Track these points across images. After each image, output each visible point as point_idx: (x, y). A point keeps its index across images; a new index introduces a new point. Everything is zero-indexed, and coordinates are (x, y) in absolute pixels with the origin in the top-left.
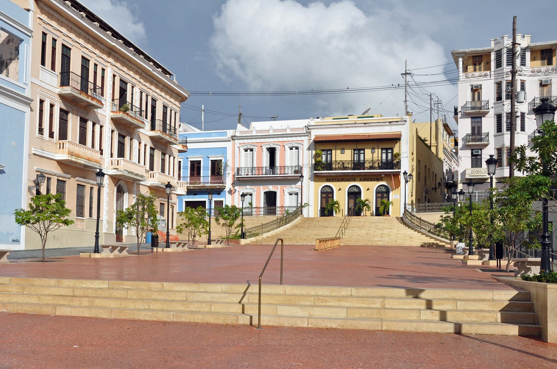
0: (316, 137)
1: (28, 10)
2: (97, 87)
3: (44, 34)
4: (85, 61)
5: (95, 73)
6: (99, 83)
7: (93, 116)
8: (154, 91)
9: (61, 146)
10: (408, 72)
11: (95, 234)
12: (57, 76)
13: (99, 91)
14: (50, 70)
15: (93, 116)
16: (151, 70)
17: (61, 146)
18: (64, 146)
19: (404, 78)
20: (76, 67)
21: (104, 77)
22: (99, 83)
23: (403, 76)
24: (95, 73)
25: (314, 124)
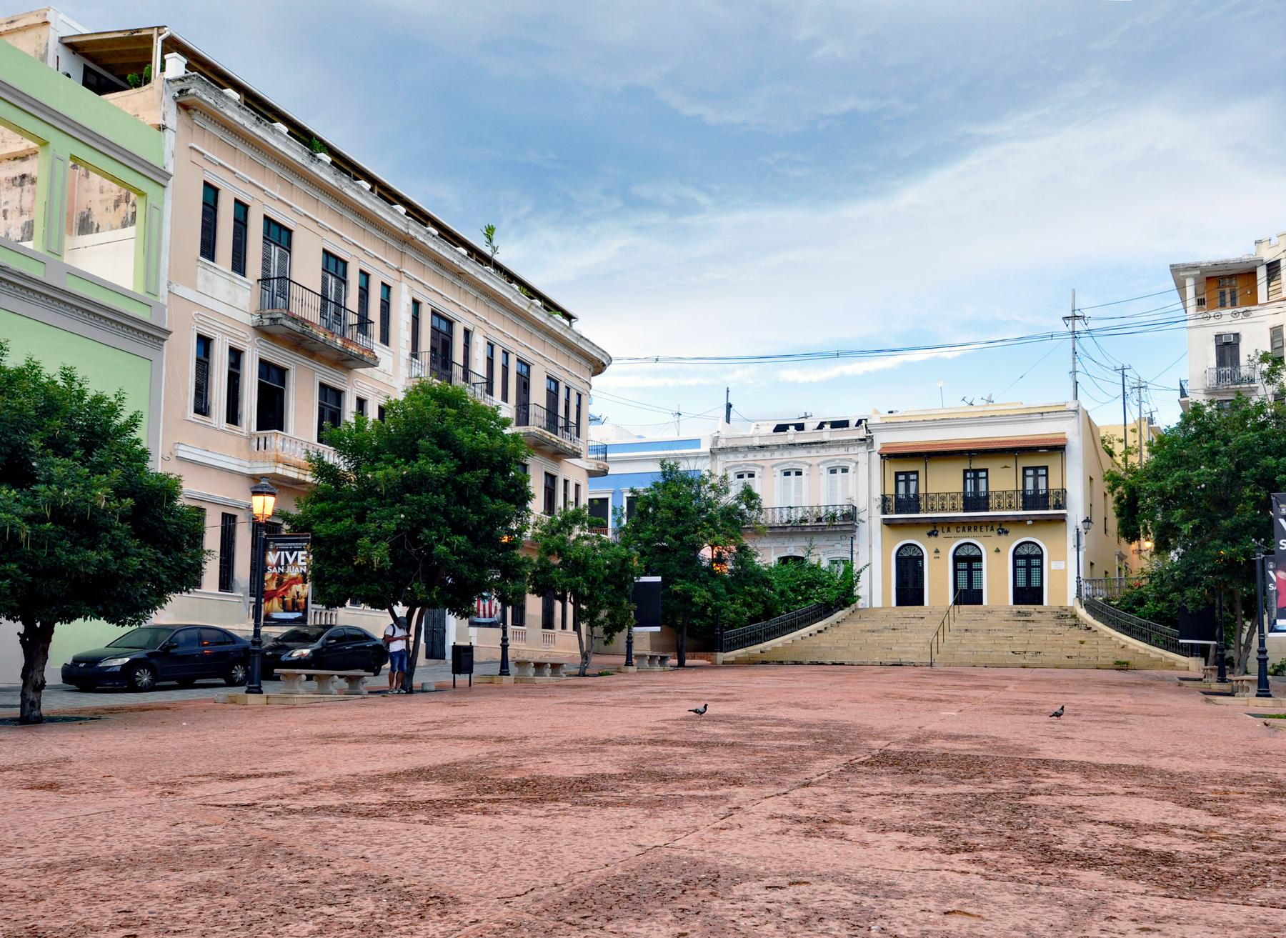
0: (884, 446)
1: (162, 128)
2: (570, 424)
3: (416, 304)
4: (334, 265)
5: (567, 401)
6: (573, 418)
7: (359, 384)
8: (522, 345)
9: (262, 443)
10: (1077, 313)
11: (501, 642)
12: (249, 288)
13: (376, 329)
14: (229, 270)
15: (359, 384)
16: (510, 297)
17: (262, 443)
18: (267, 442)
19: (1070, 326)
20: (538, 395)
21: (388, 304)
22: (573, 418)
23: (1067, 321)
24: (567, 401)
25: (878, 421)
